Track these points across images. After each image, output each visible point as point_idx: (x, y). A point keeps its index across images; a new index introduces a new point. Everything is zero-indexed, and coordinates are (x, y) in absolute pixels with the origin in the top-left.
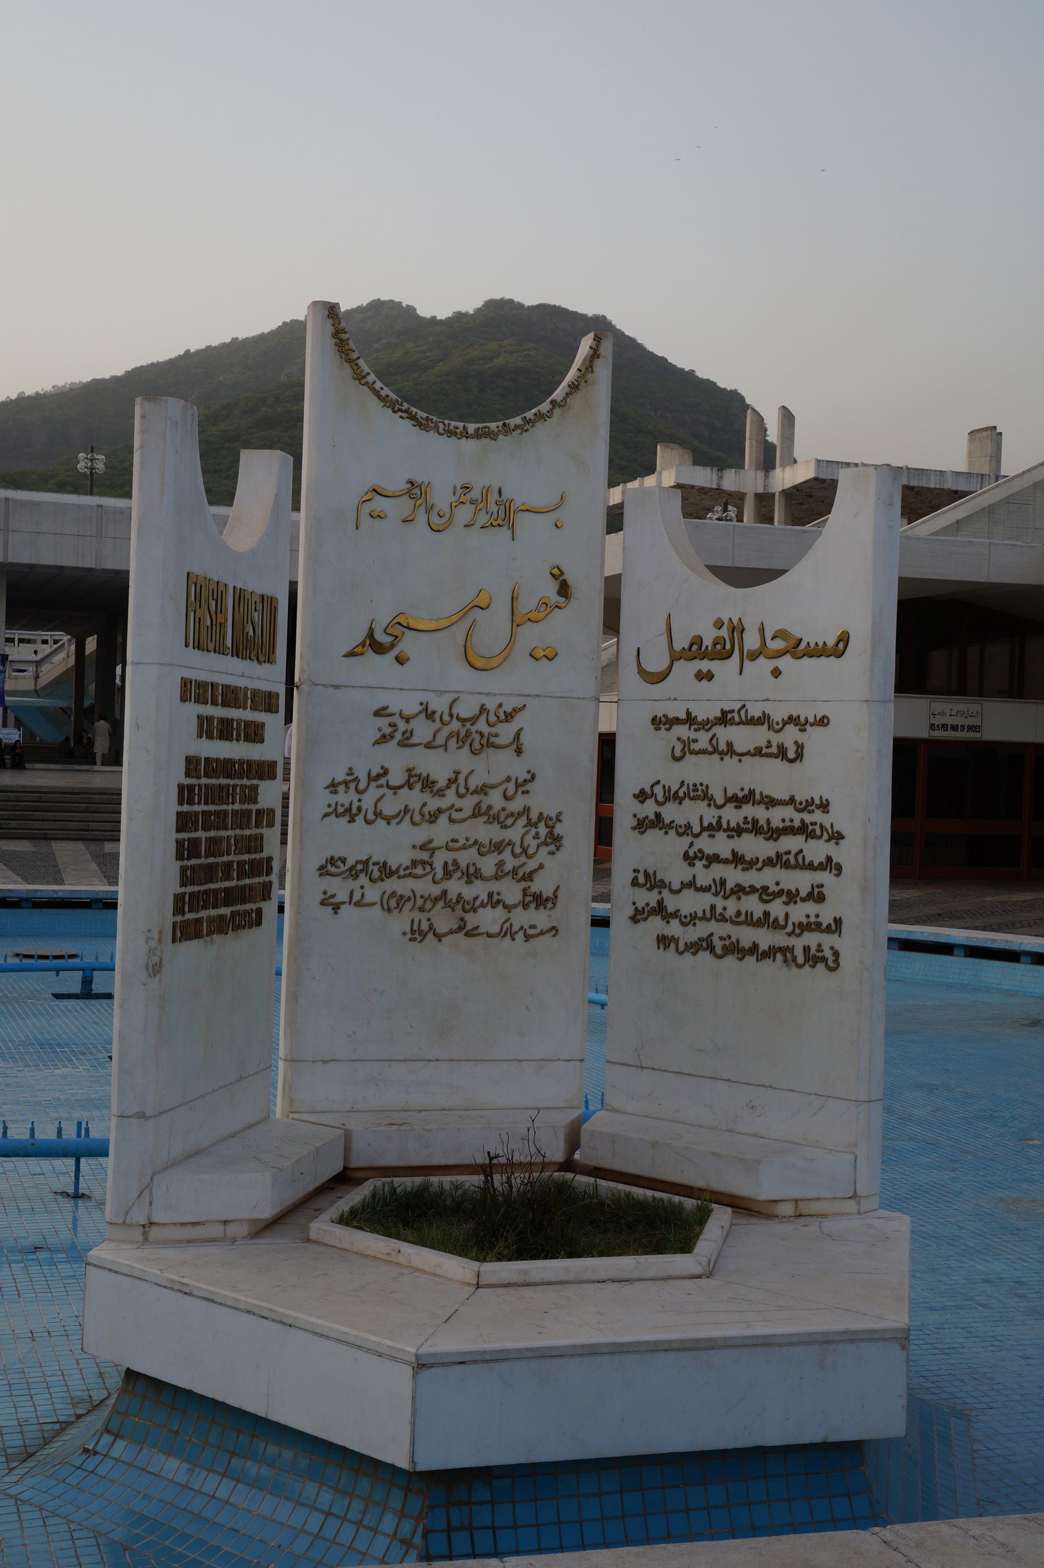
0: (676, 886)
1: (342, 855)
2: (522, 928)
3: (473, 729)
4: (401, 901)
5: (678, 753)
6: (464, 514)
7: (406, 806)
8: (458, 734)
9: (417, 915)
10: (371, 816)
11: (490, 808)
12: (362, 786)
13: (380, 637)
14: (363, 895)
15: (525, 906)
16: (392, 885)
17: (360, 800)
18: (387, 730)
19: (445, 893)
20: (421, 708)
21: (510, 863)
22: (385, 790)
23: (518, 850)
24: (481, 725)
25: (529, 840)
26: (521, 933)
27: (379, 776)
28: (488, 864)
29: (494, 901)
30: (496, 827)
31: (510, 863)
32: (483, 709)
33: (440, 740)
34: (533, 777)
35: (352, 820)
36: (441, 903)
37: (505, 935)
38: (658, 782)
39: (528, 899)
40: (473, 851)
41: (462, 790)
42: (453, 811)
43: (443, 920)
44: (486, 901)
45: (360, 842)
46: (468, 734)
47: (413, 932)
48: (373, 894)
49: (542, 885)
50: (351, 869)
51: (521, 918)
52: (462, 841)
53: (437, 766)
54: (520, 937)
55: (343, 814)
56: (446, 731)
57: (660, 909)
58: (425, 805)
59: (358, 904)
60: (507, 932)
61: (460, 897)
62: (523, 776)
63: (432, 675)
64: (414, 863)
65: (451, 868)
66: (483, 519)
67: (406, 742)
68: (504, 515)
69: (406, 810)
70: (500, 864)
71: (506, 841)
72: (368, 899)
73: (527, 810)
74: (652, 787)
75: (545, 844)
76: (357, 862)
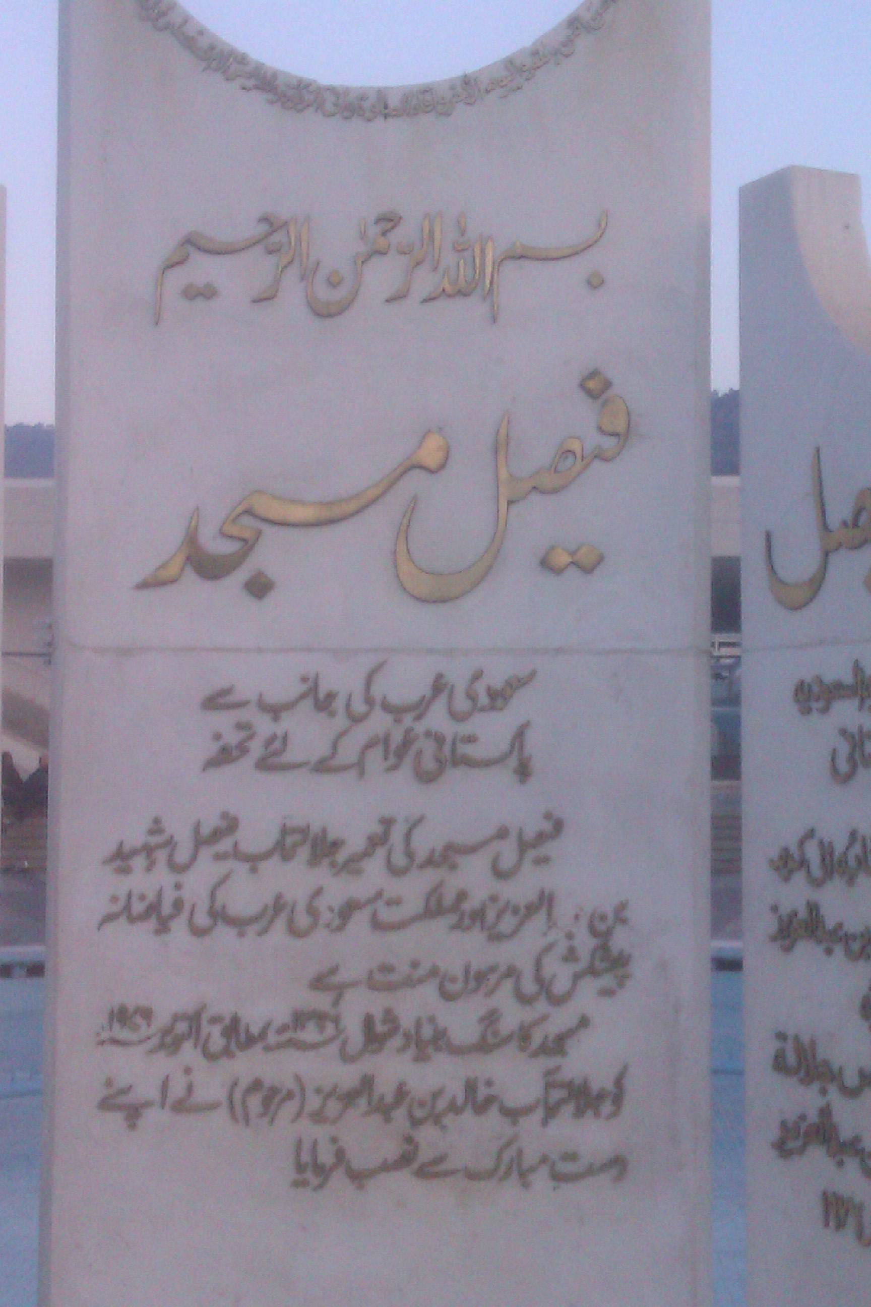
0: (851, 1079)
1: (143, 1002)
2: (544, 1160)
3: (420, 728)
4: (272, 1097)
5: (843, 766)
6: (382, 276)
7: (279, 897)
8: (386, 741)
9: (308, 1130)
10: (202, 919)
11: (462, 896)
12: (182, 856)
13: (215, 545)
14: (190, 1089)
15: (551, 1111)
16: (248, 1065)
17: (178, 886)
18: (232, 738)
19: (367, 1082)
20: (303, 688)
21: (513, 1016)
22: (231, 864)
23: (529, 986)
24: (437, 718)
25: (554, 967)
26: (544, 1170)
27: (217, 835)
29: (478, 1099)
30: (475, 939)
31: (513, 1016)
32: (439, 686)
33: (348, 753)
34: (558, 826)
35: (163, 928)
36: (363, 1102)
37: (507, 1174)
38: (810, 834)
39: (557, 1095)
40: (429, 991)
41: (399, 860)
42: (380, 904)
43: (367, 1138)
44: (460, 1100)
46: (408, 741)
47: (300, 1168)
48: (211, 1084)
49: (588, 1061)
50: (167, 1031)
51: (536, 1138)
52: (404, 969)
53: (345, 808)
54: (541, 1180)
55: (144, 916)
56: (360, 735)
57: (821, 1132)
58: (318, 892)
59: (181, 1107)
60: (512, 1168)
61: (401, 1093)
62: (533, 826)
64: (299, 1019)
65: (380, 1028)
66: (425, 282)
67: (270, 763)
69: (278, 905)
70: (491, 1018)
71: (503, 968)
72: (201, 1095)
73: (545, 901)
74: (802, 843)
75: (592, 971)
76: (176, 1018)
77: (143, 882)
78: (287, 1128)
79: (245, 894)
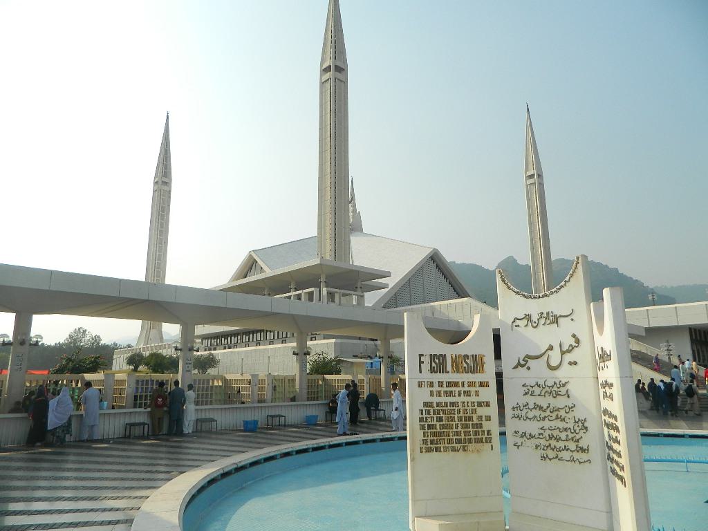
6: (542, 321)
10: (525, 418)
11: (561, 416)
19: (550, 445)
23: (573, 431)
24: (555, 388)
25: (576, 428)
27: (526, 406)
28: (563, 436)
32: (555, 383)
33: (543, 394)
36: (549, 448)
43: (551, 454)
45: (524, 426)
46: (551, 391)
49: (583, 444)
51: (576, 455)
53: (544, 402)
60: (572, 460)
61: (555, 447)
62: (571, 405)
63: (538, 371)
68: (556, 320)
77: (517, 412)
78: (540, 452)
79: (531, 415)
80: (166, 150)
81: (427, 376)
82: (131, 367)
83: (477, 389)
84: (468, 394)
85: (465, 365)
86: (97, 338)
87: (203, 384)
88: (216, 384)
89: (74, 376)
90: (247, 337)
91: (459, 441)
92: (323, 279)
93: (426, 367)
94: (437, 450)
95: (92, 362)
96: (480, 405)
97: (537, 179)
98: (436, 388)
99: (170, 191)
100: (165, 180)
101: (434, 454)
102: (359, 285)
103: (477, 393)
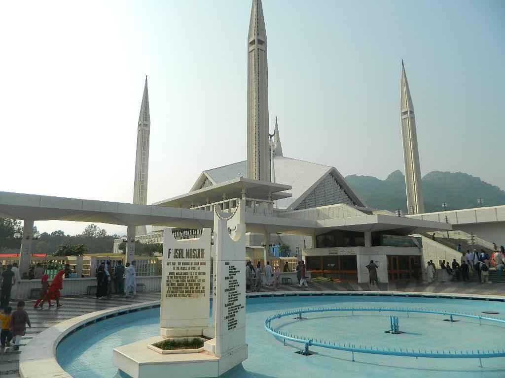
80: (146, 102)
81: (172, 259)
82: (121, 251)
83: (199, 266)
84: (193, 268)
85: (193, 254)
86: (104, 232)
87: (141, 262)
88: (152, 263)
89: (61, 258)
90: (188, 232)
91: (187, 292)
92: (243, 191)
93: (172, 255)
94: (175, 296)
95: (78, 249)
96: (200, 274)
97: (410, 114)
98: (177, 265)
99: (149, 131)
100: (145, 123)
101: (173, 298)
102: (270, 195)
103: (199, 268)
